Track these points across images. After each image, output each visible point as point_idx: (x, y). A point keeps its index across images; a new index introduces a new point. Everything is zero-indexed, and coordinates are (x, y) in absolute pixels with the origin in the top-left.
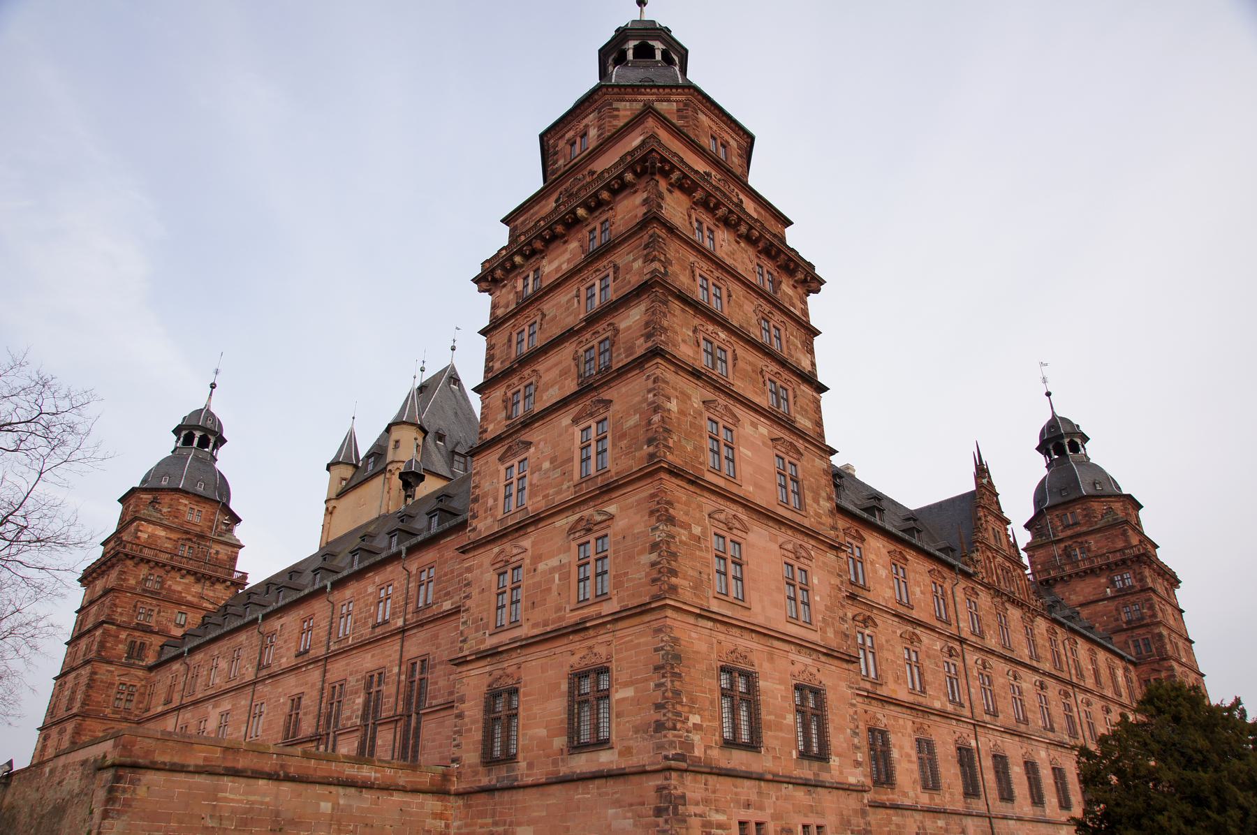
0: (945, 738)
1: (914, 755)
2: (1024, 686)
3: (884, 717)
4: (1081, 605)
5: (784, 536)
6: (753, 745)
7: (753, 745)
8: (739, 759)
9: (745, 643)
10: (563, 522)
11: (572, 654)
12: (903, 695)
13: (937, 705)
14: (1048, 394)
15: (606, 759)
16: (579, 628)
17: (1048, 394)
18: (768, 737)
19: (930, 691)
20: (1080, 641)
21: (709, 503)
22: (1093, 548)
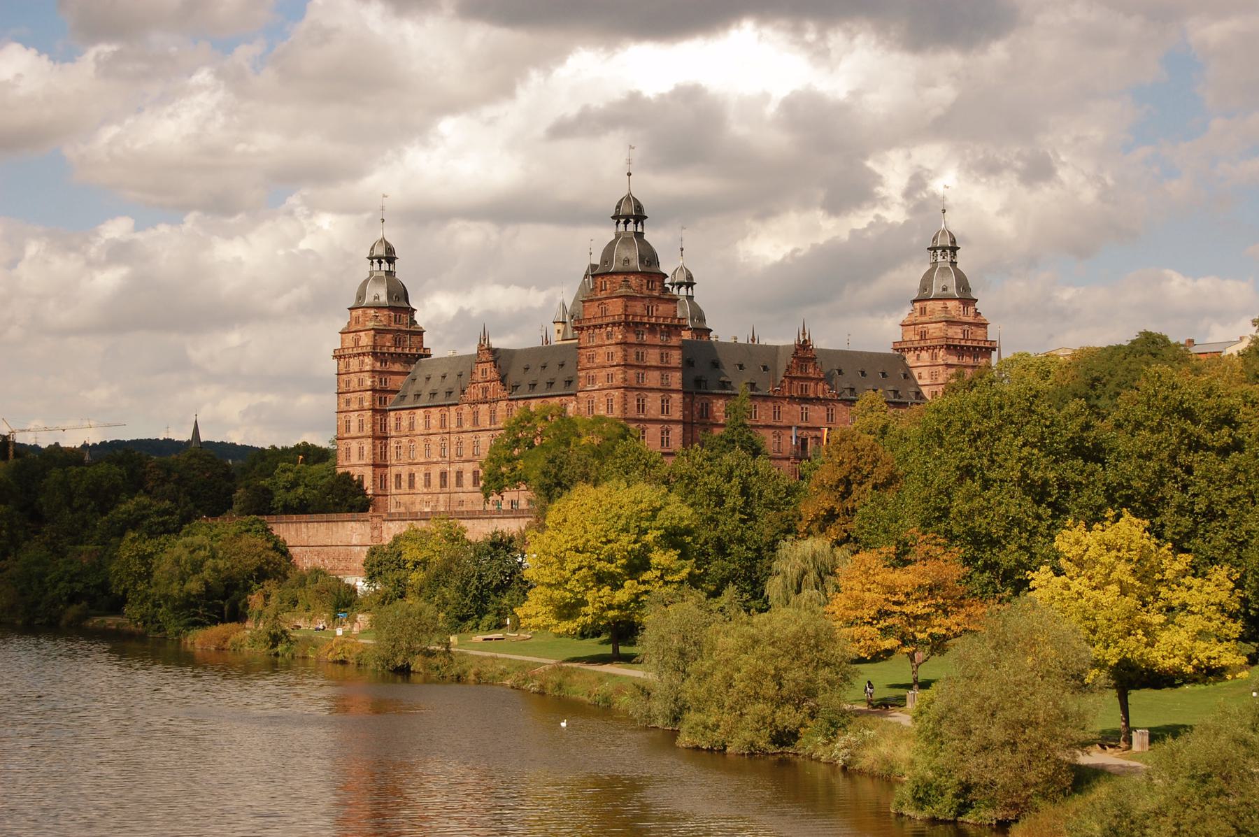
0: (435, 472)
1: (423, 478)
3: (414, 469)
5: (358, 440)
12: (422, 460)
13: (435, 460)
17: (629, 174)
19: (432, 456)
21: (345, 441)
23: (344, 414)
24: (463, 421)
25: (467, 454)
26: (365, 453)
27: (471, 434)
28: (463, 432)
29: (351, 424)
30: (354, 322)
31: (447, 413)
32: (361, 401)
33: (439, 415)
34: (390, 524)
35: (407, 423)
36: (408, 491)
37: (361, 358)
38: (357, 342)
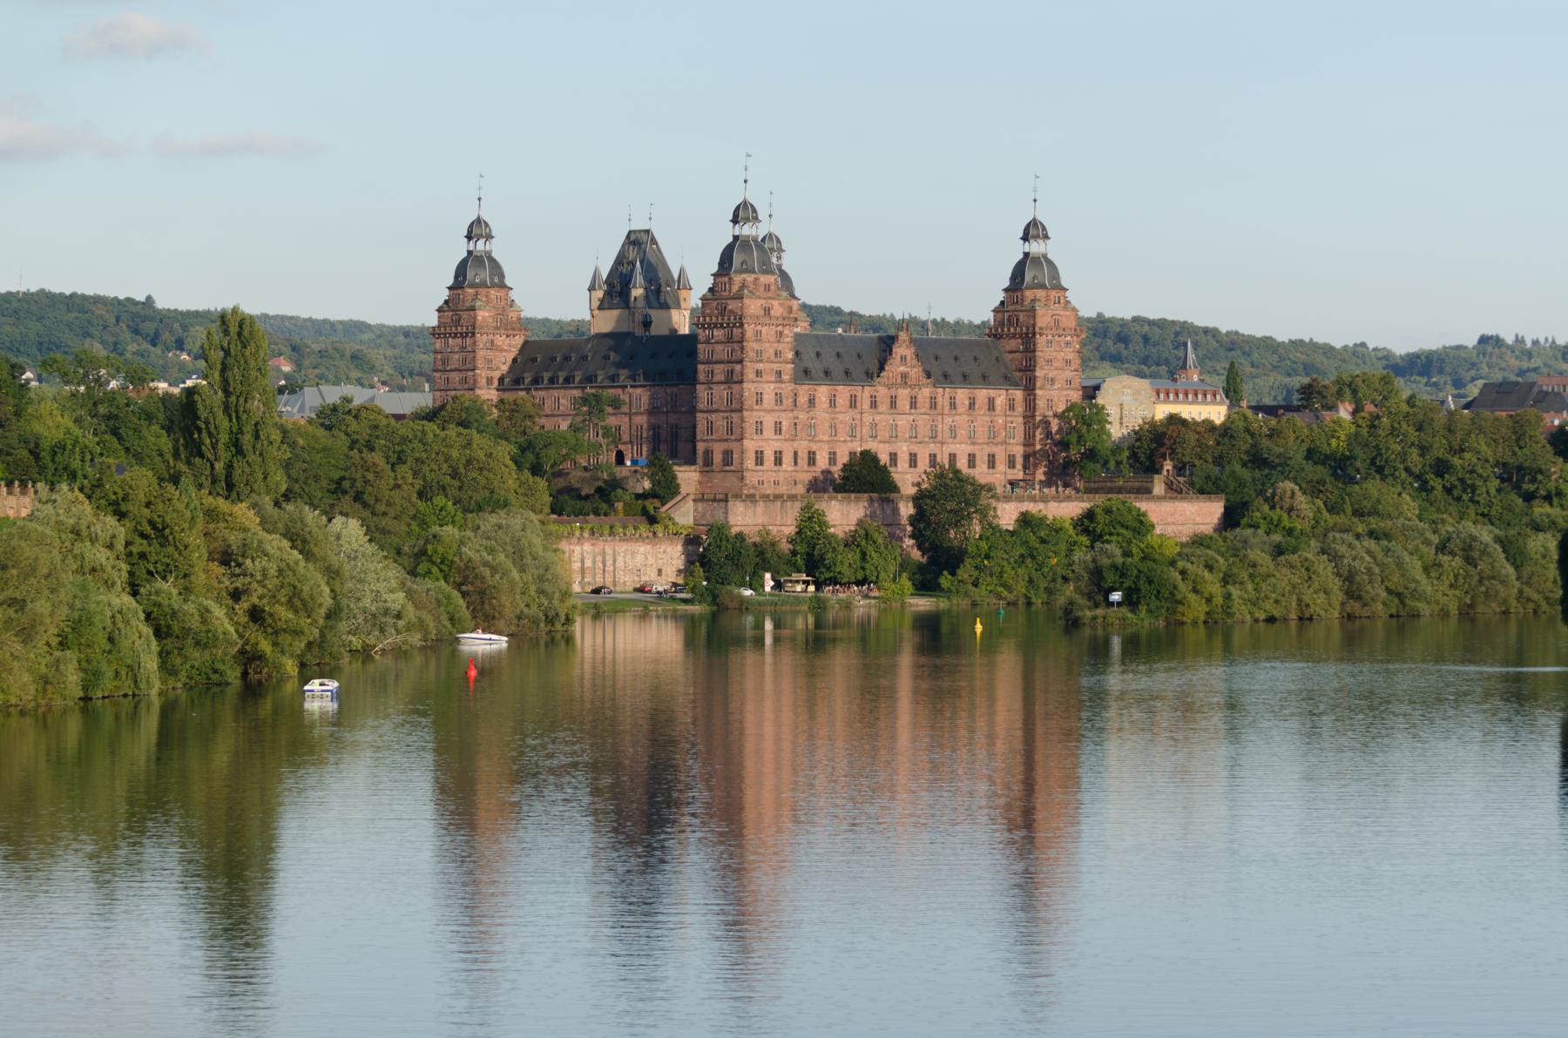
1: (827, 457)
2: (900, 423)
4: (1010, 352)
6: (762, 464)
7: (762, 464)
8: (759, 468)
9: (761, 444)
10: (722, 414)
11: (725, 446)
12: (826, 438)
13: (842, 439)
14: (1035, 201)
15: (732, 468)
16: (726, 440)
17: (1035, 201)
18: (766, 463)
20: (960, 391)
21: (755, 414)
22: (1021, 320)
23: (755, 385)
24: (878, 404)
25: (884, 434)
26: (784, 428)
27: (888, 417)
28: (880, 413)
29: (765, 396)
30: (762, 289)
31: (859, 394)
32: (779, 373)
33: (848, 395)
34: (1006, 506)
35: (806, 399)
36: (806, 468)
37: (780, 328)
38: (767, 311)
